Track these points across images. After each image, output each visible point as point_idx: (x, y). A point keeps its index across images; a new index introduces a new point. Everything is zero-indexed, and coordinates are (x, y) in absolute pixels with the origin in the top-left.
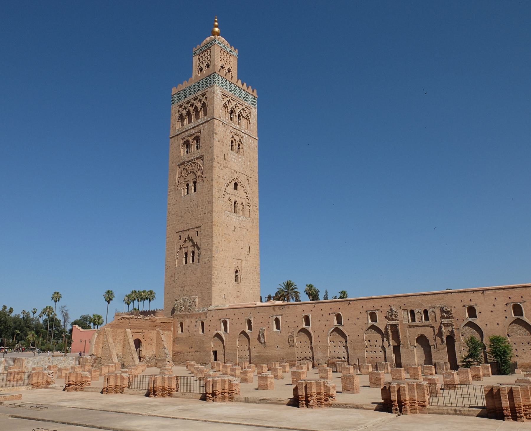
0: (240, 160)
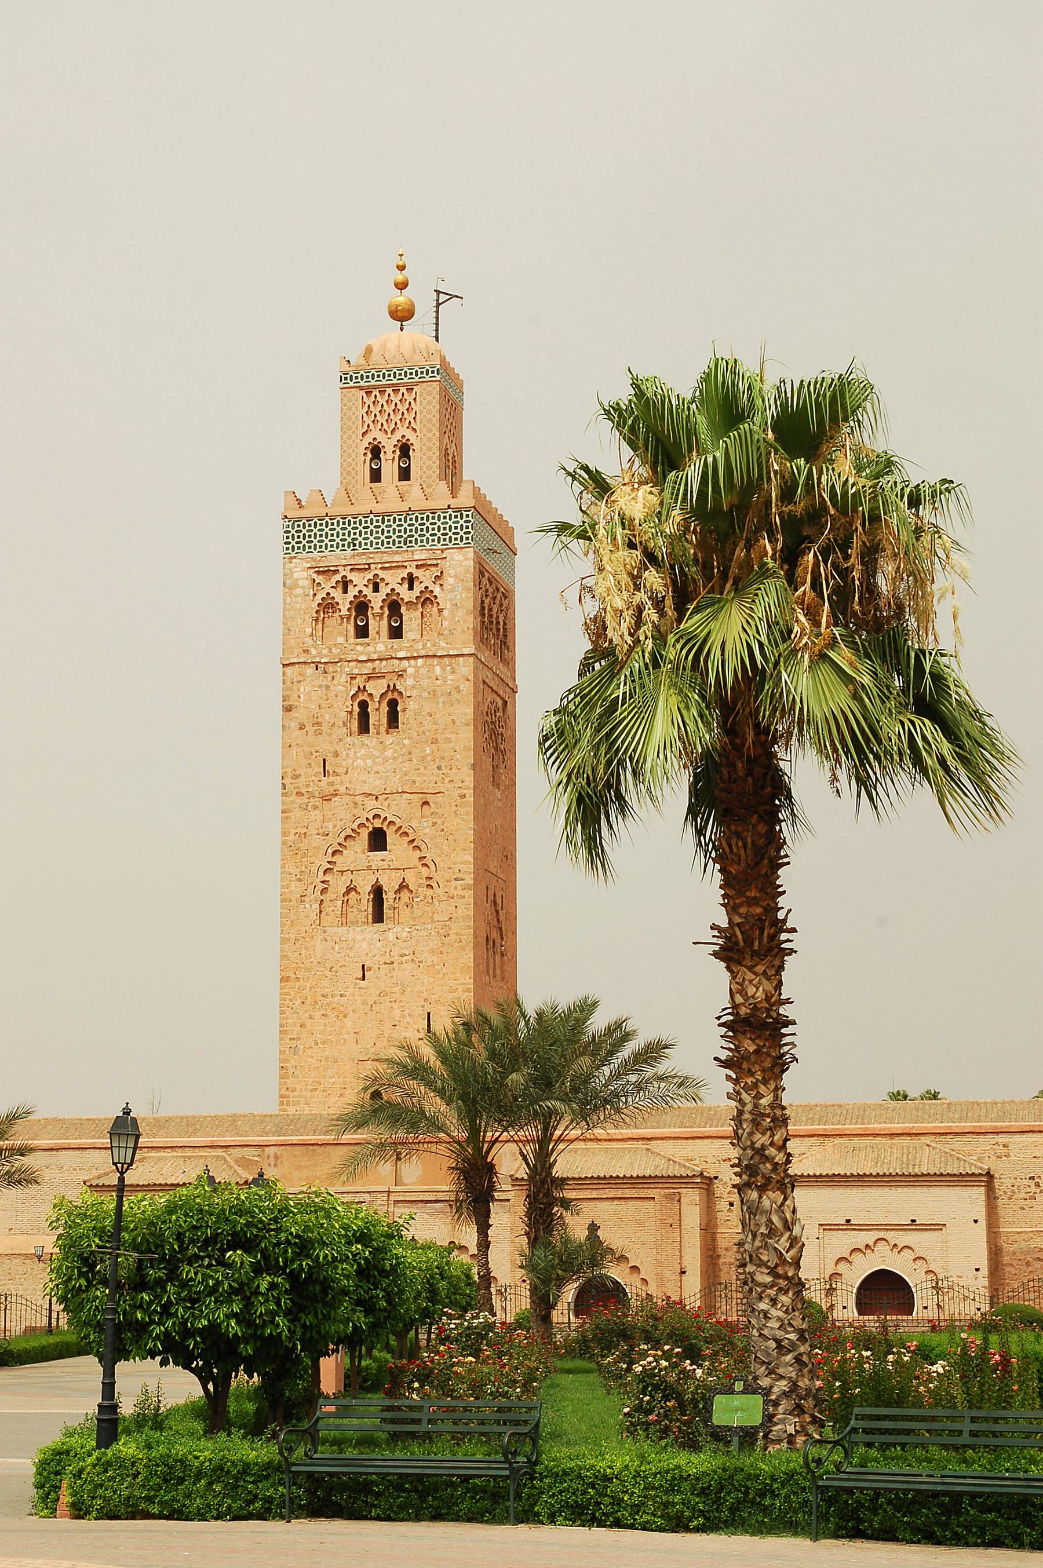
0: (389, 753)
